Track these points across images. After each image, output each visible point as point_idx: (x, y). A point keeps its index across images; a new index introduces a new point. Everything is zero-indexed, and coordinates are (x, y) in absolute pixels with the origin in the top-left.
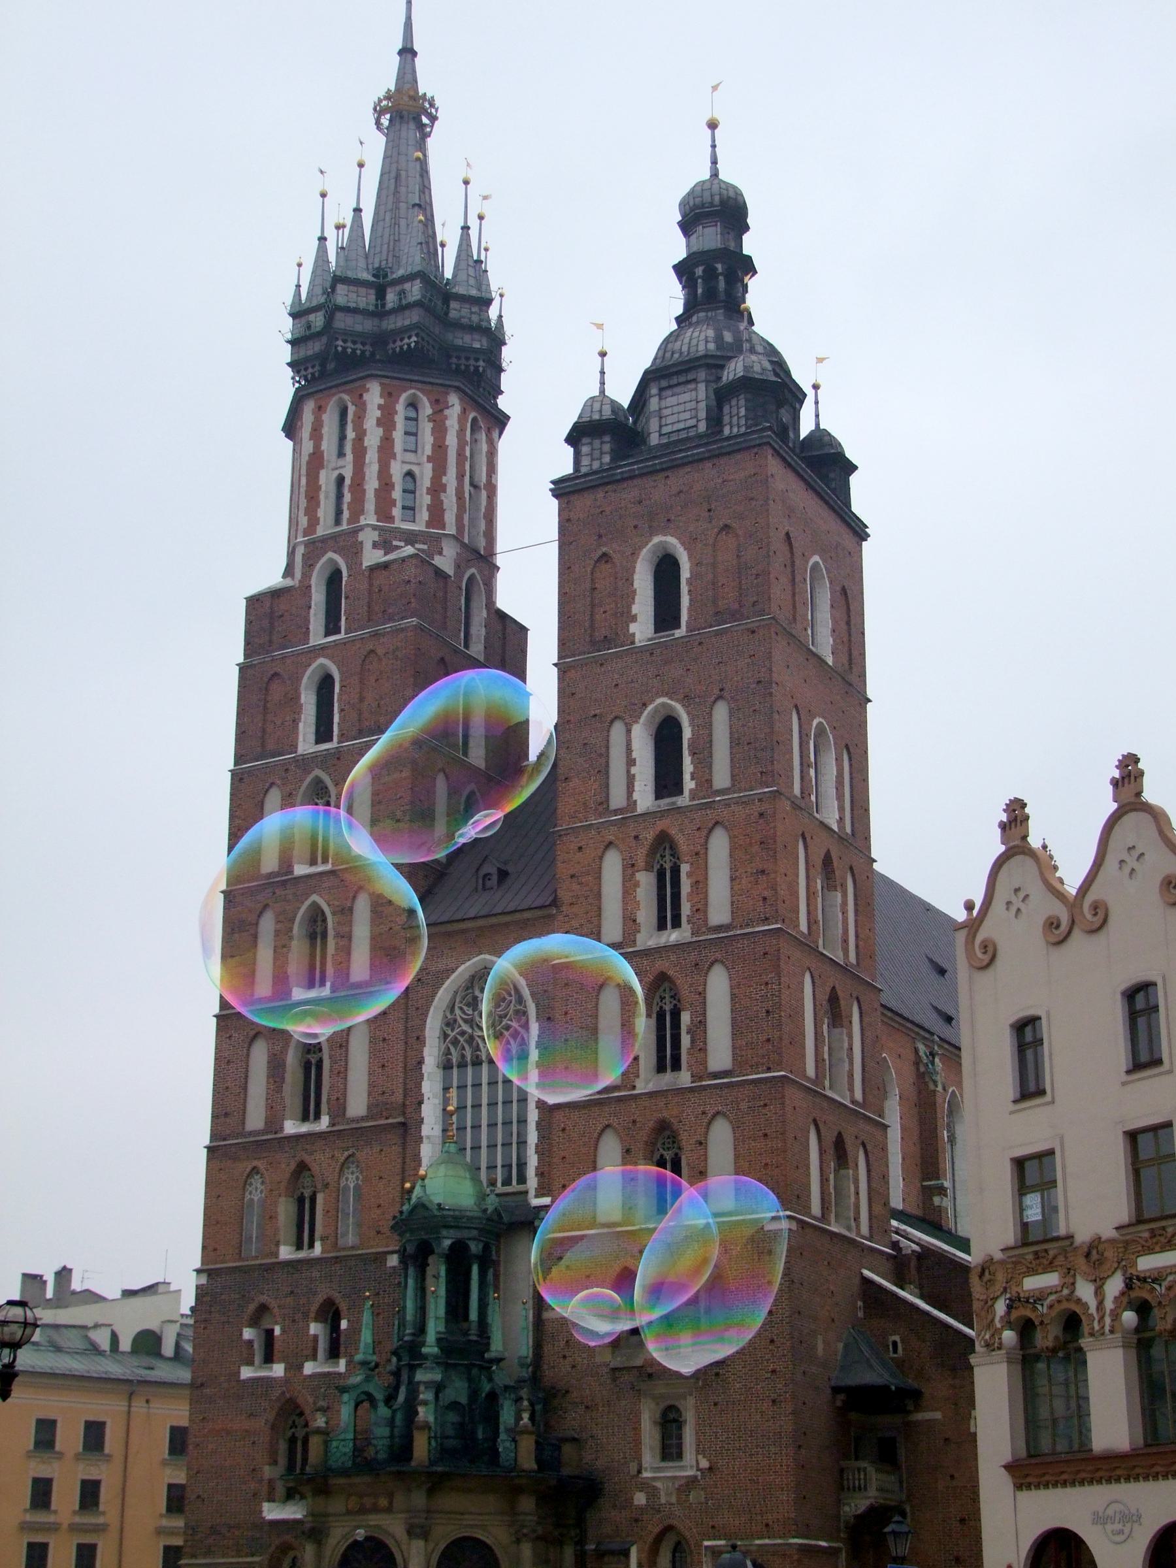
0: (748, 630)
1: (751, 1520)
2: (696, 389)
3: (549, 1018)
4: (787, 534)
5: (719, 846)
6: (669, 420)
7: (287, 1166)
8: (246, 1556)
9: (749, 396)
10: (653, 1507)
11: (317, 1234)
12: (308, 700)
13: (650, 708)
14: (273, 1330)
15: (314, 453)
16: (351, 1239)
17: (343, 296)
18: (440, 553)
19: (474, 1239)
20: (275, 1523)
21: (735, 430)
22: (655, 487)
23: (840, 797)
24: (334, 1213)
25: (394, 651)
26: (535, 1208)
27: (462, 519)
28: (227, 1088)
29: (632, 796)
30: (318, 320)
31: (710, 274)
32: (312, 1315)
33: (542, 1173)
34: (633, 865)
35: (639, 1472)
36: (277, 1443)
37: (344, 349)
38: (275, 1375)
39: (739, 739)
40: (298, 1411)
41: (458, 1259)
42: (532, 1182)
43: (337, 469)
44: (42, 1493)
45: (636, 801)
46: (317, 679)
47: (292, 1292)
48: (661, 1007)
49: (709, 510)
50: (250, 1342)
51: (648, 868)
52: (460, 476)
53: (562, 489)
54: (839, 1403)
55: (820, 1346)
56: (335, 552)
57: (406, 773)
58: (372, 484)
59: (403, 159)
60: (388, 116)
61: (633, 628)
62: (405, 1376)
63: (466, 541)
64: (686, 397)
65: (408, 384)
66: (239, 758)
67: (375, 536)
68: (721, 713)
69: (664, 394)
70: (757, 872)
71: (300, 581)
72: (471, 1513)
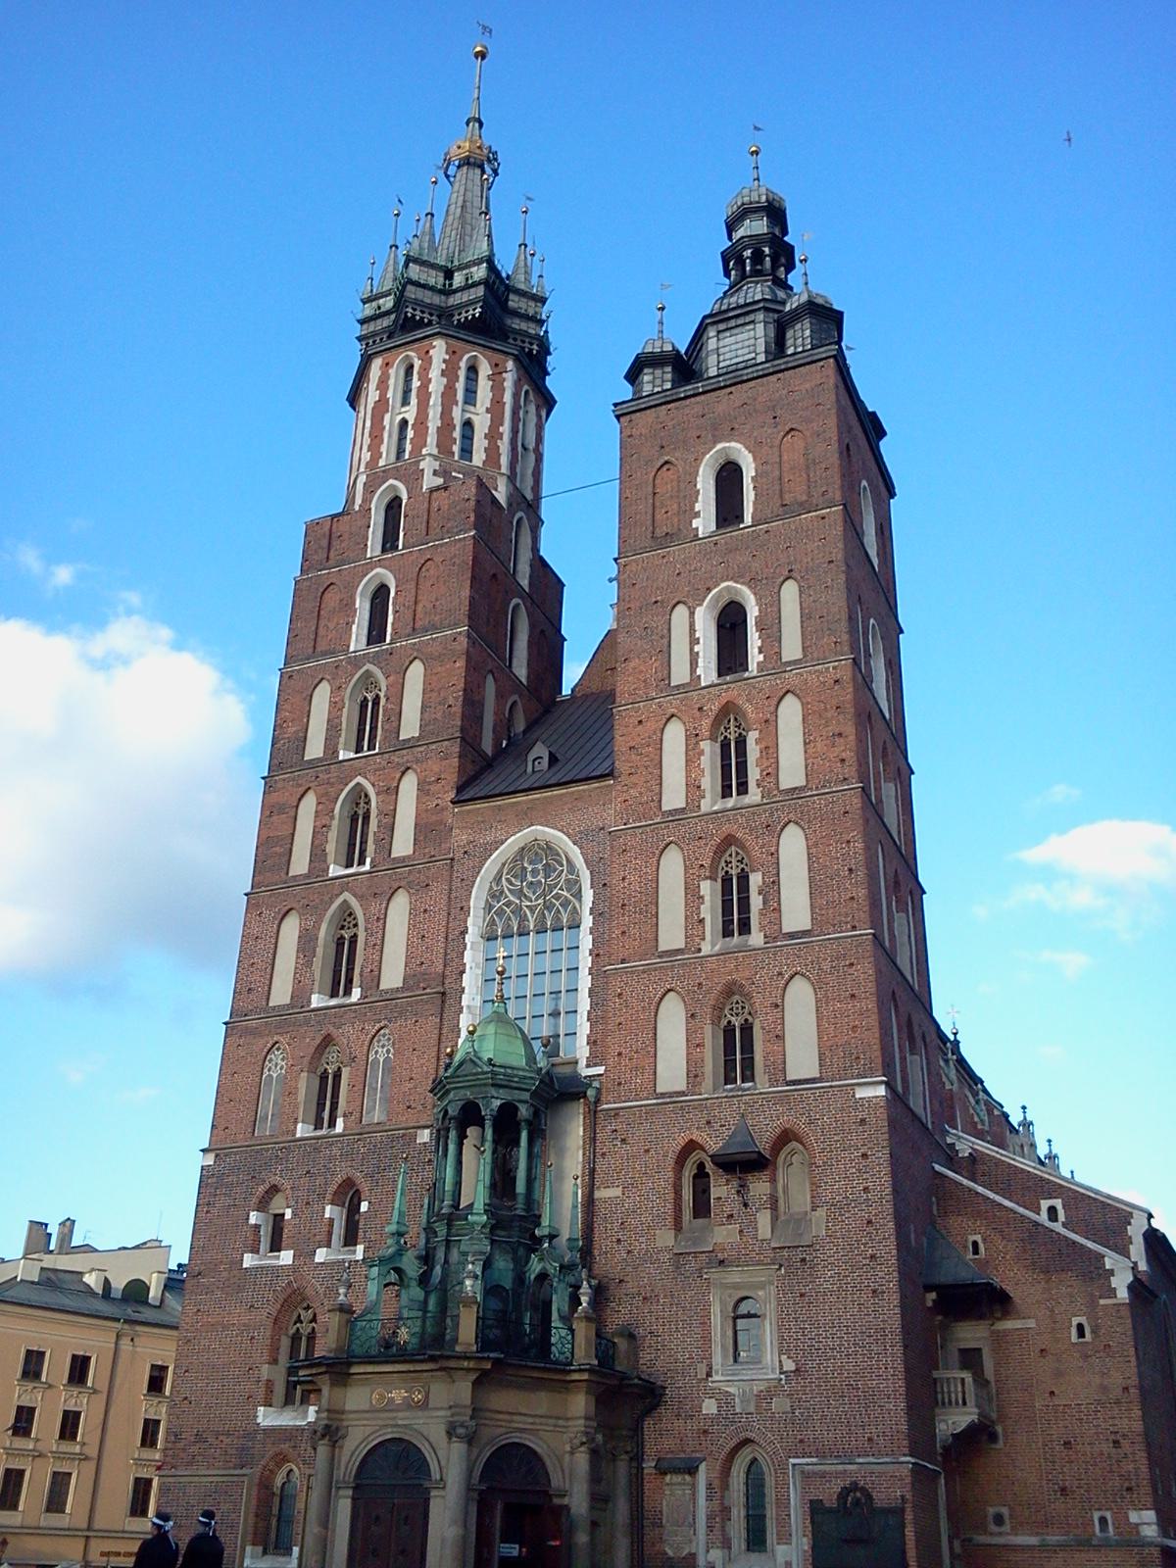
0: (817, 516)
1: (850, 1432)
2: (754, 329)
3: (605, 885)
4: (848, 445)
5: (790, 712)
6: (727, 356)
7: (312, 1041)
8: (235, 1468)
9: (814, 321)
10: (727, 1413)
11: (340, 1111)
12: (362, 606)
13: (714, 592)
14: (283, 1215)
15: (379, 401)
16: (377, 1116)
17: (414, 272)
18: (496, 490)
19: (525, 1102)
20: (270, 1431)
21: (800, 349)
22: (718, 402)
23: (888, 700)
24: (361, 1086)
25: (451, 559)
26: (585, 1077)
27: (515, 468)
28: (253, 964)
29: (695, 672)
30: (388, 303)
31: (758, 257)
32: (329, 1197)
33: (595, 1041)
34: (697, 735)
35: (709, 1375)
36: (279, 1340)
37: (414, 316)
38: (281, 1263)
39: (810, 613)
40: (305, 1305)
41: (506, 1125)
42: (582, 1051)
43: (400, 413)
44: (23, 1422)
45: (699, 676)
46: (372, 587)
47: (308, 1172)
48: (727, 872)
49: (775, 418)
50: (257, 1227)
51: (713, 738)
52: (515, 431)
53: (622, 412)
54: (930, 1304)
55: (913, 1236)
56: (396, 479)
57: (461, 663)
58: (434, 422)
59: (469, 194)
60: (457, 163)
61: (695, 523)
62: (440, 1255)
63: (518, 485)
64: (745, 336)
65: (468, 347)
66: (289, 660)
67: (436, 465)
68: (790, 592)
69: (721, 336)
70: (833, 735)
71: (360, 506)
72: (521, 1414)
